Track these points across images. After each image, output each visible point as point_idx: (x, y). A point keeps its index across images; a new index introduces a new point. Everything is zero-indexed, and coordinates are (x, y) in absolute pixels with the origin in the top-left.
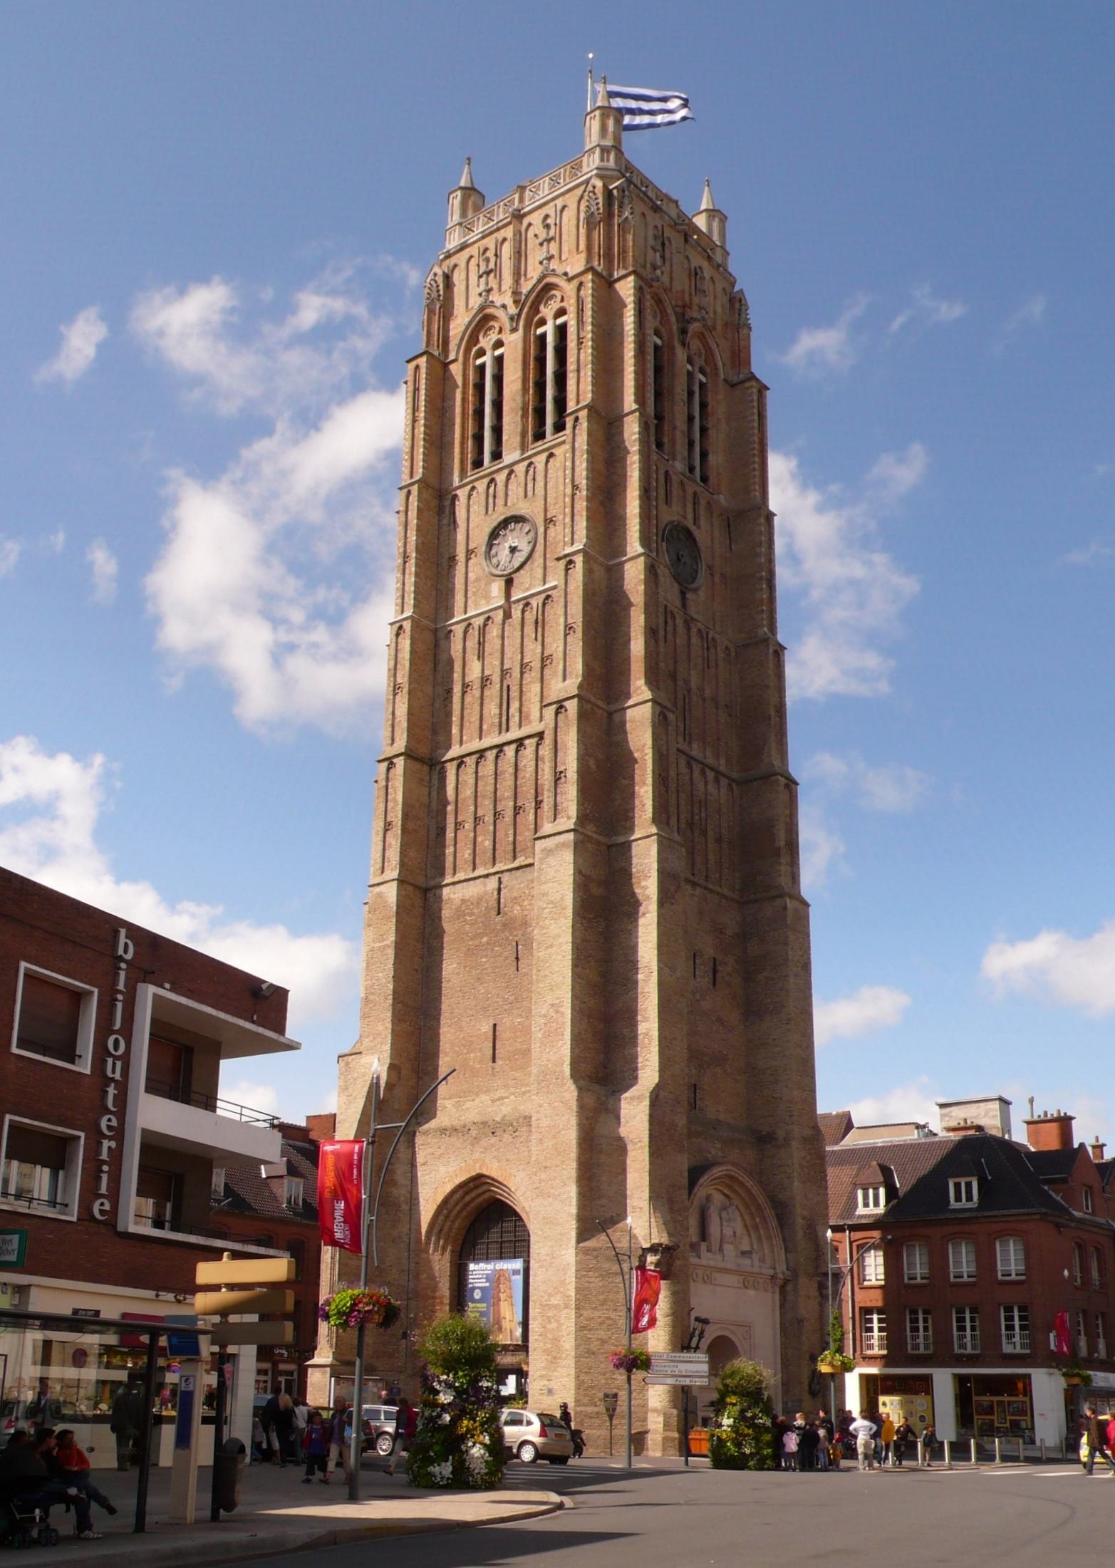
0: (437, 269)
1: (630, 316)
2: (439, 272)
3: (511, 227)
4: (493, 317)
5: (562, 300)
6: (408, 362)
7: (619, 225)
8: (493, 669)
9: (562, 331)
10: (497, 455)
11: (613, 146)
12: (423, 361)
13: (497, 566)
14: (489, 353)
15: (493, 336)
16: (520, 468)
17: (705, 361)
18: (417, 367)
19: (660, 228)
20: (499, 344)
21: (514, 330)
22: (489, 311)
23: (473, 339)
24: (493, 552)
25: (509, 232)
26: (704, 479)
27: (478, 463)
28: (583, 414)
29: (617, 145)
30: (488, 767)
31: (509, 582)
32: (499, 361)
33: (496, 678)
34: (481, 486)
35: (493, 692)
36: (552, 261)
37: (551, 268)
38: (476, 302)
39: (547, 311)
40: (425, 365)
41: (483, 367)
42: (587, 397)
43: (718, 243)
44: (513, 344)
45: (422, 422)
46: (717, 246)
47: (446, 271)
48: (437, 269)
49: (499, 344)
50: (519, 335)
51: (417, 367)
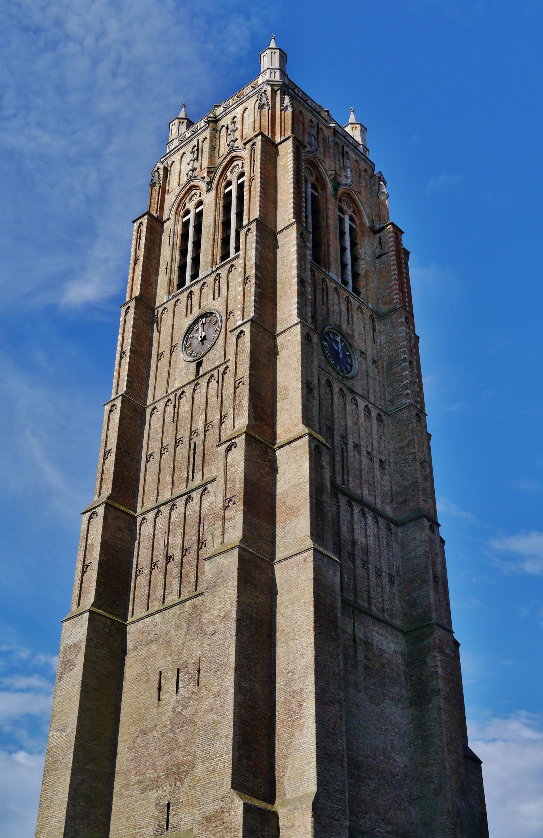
0: (159, 165)
1: (290, 161)
2: (162, 167)
3: (208, 130)
4: (195, 187)
5: (242, 167)
6: (134, 222)
7: (281, 111)
8: (184, 433)
9: (241, 187)
10: (195, 276)
11: (277, 69)
12: (145, 220)
13: (191, 354)
14: (192, 212)
15: (196, 200)
16: (210, 280)
17: (353, 212)
18: (141, 223)
19: (315, 124)
20: (200, 203)
21: (208, 190)
22: (192, 183)
23: (181, 202)
24: (189, 343)
25: (207, 133)
26: (356, 291)
27: (181, 283)
28: (253, 227)
29: (282, 69)
30: (177, 514)
31: (199, 364)
32: (199, 216)
33: (186, 440)
34: (183, 297)
35: (183, 451)
36: (236, 142)
37: (236, 145)
38: (184, 179)
39: (232, 176)
40: (146, 221)
41: (188, 221)
42: (256, 214)
43: (360, 142)
44: (209, 198)
45: (142, 259)
46: (360, 145)
47: (166, 166)
48: (159, 165)
49: (200, 203)
50: (213, 193)
51: (141, 223)
